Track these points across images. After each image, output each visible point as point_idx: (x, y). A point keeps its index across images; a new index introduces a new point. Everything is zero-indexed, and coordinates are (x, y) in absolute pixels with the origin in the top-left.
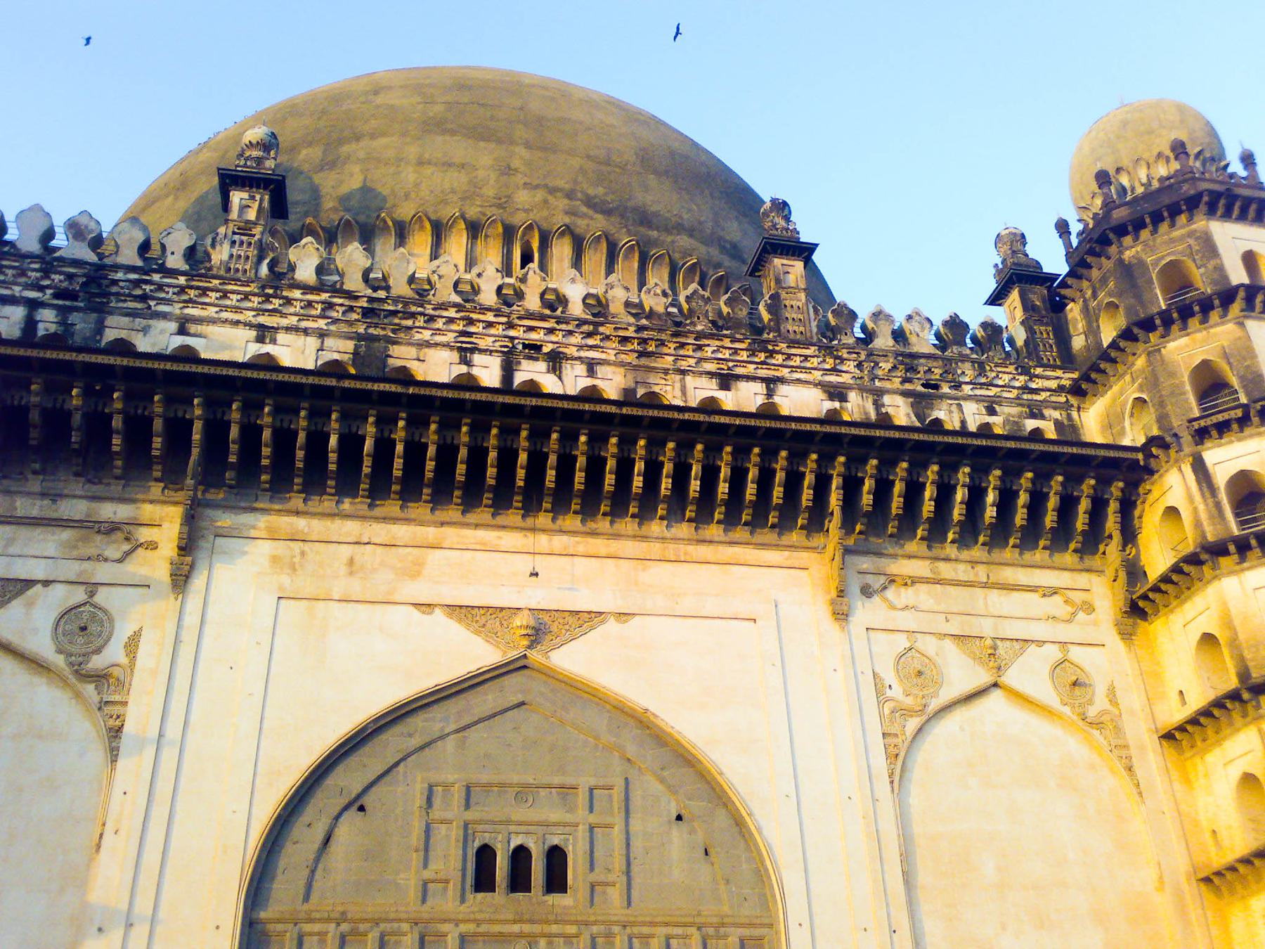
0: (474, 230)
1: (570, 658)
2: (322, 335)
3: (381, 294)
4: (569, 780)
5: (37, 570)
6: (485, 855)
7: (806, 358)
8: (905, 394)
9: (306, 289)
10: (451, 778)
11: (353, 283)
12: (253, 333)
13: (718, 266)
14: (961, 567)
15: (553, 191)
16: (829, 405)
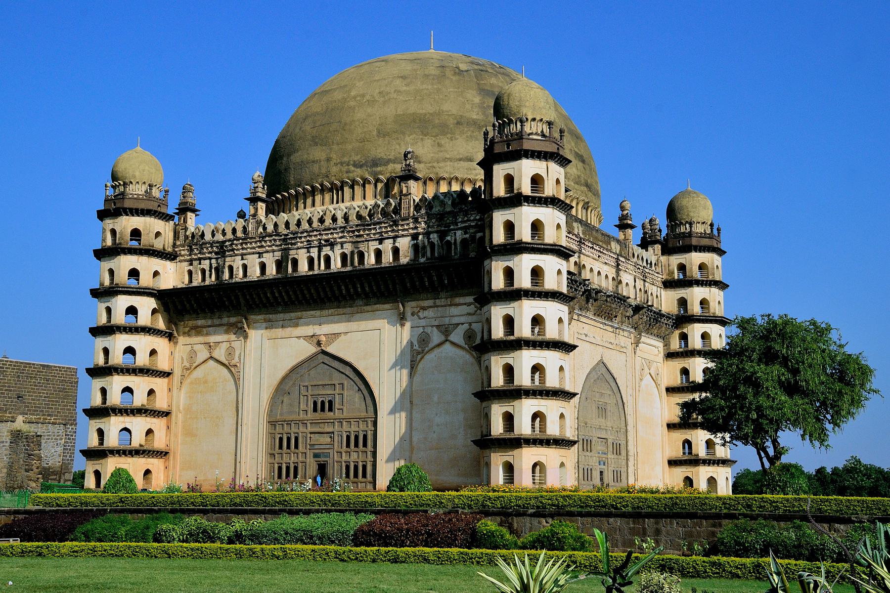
2: (273, 251)
6: (315, 403)
7: (408, 224)
8: (436, 232)
11: (282, 229)
15: (342, 164)
16: (412, 242)
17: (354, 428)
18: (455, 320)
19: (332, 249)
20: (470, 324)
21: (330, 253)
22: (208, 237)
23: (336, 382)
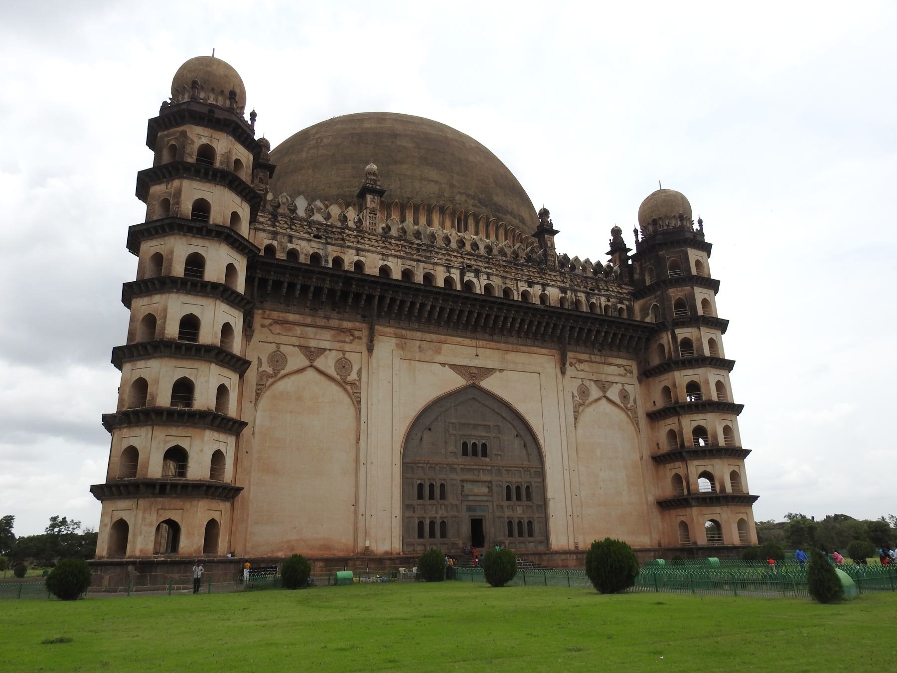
0: (442, 211)
1: (487, 384)
2: (402, 258)
3: (419, 242)
4: (488, 423)
5: (327, 345)
6: (465, 445)
8: (584, 292)
9: (396, 239)
10: (454, 421)
12: (380, 257)
13: (518, 228)
14: (598, 357)
15: (468, 195)
16: (561, 295)
17: (515, 479)
18: (611, 379)
19: (477, 276)
20: (623, 384)
21: (475, 280)
22: (301, 212)
23: (491, 424)
